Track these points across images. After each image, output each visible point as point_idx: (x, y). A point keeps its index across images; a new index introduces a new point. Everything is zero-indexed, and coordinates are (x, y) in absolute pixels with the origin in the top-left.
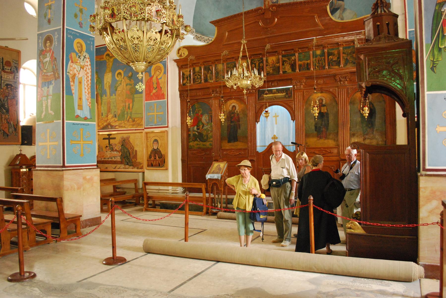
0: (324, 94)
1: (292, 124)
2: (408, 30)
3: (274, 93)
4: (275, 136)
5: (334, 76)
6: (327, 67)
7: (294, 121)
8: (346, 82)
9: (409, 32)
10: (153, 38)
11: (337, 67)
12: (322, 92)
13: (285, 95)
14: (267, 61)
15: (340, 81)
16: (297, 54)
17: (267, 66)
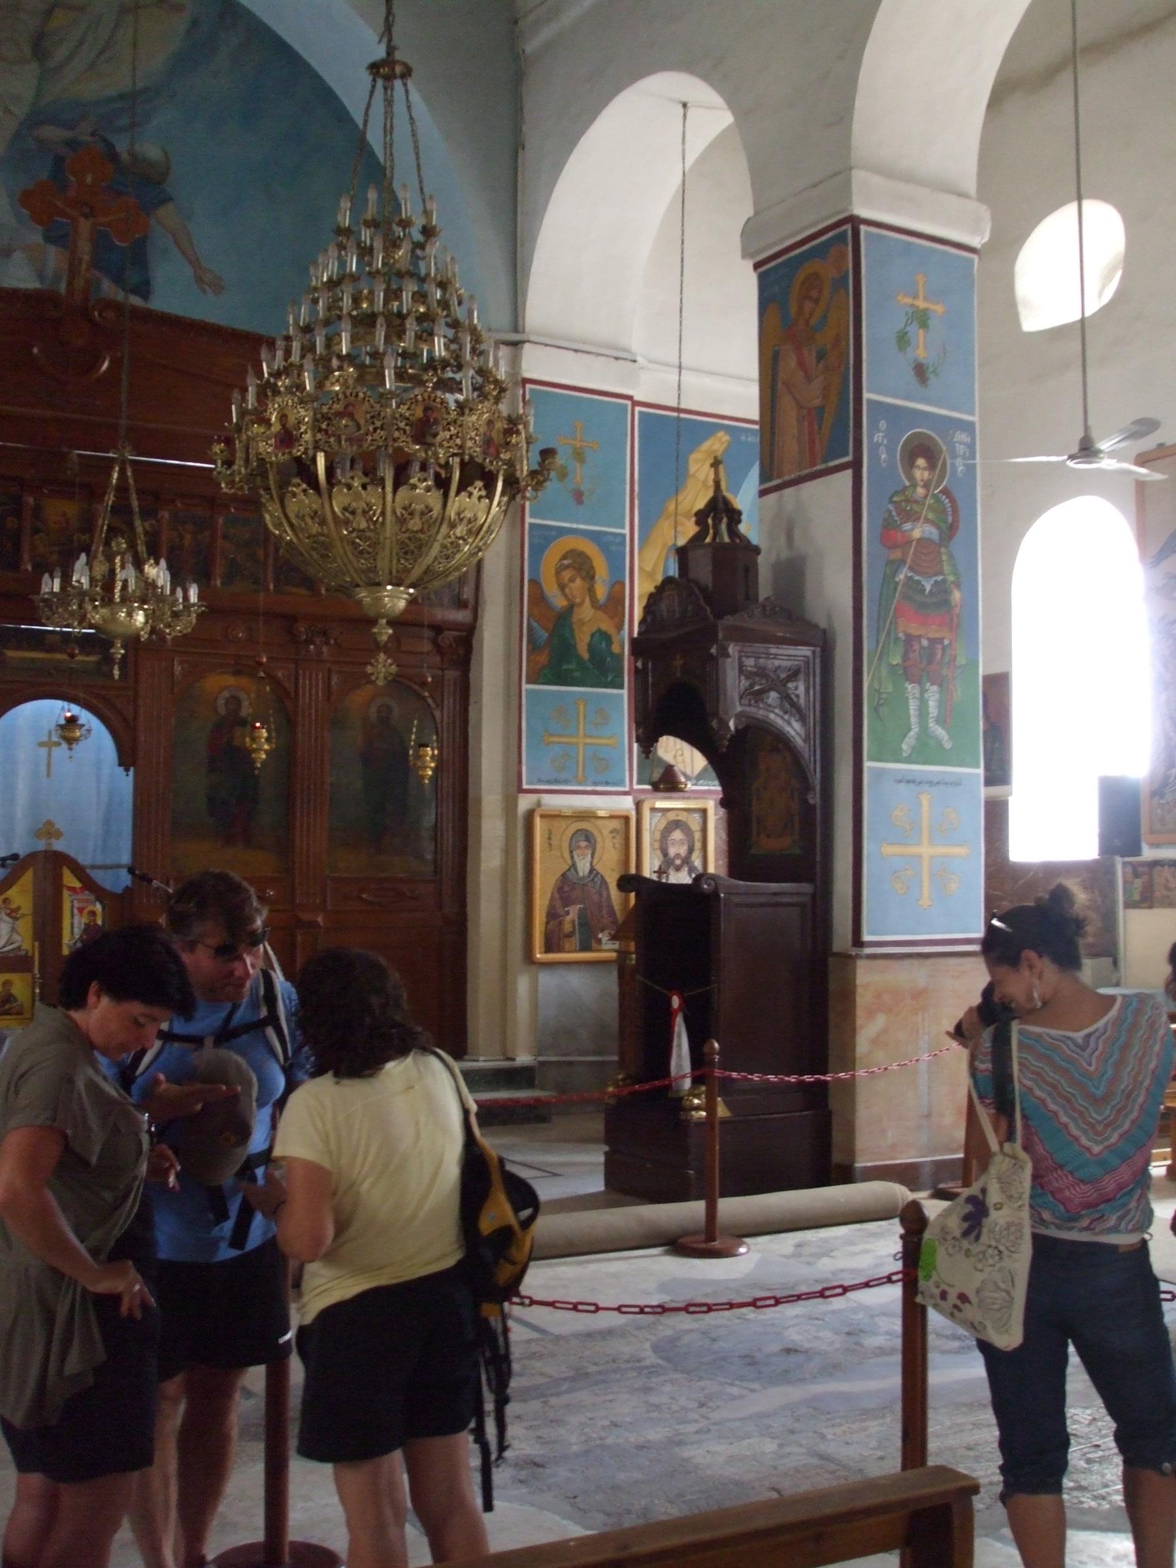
0: (244, 681)
1: (125, 782)
2: (528, 520)
3: (51, 649)
4: (49, 823)
5: (291, 619)
6: (271, 586)
7: (127, 770)
8: (325, 649)
9: (531, 525)
10: (418, 507)
11: (303, 591)
12: (237, 673)
13: (98, 663)
14: (37, 510)
15: (309, 641)
16: (165, 515)
17: (36, 531)
